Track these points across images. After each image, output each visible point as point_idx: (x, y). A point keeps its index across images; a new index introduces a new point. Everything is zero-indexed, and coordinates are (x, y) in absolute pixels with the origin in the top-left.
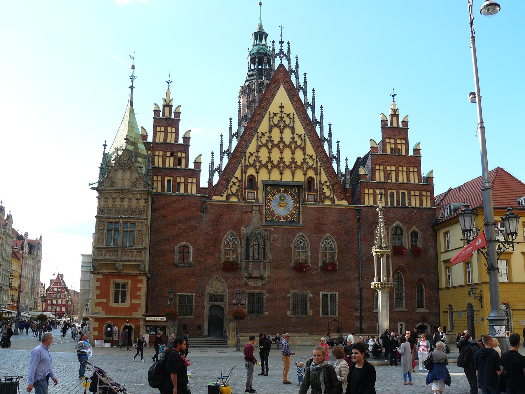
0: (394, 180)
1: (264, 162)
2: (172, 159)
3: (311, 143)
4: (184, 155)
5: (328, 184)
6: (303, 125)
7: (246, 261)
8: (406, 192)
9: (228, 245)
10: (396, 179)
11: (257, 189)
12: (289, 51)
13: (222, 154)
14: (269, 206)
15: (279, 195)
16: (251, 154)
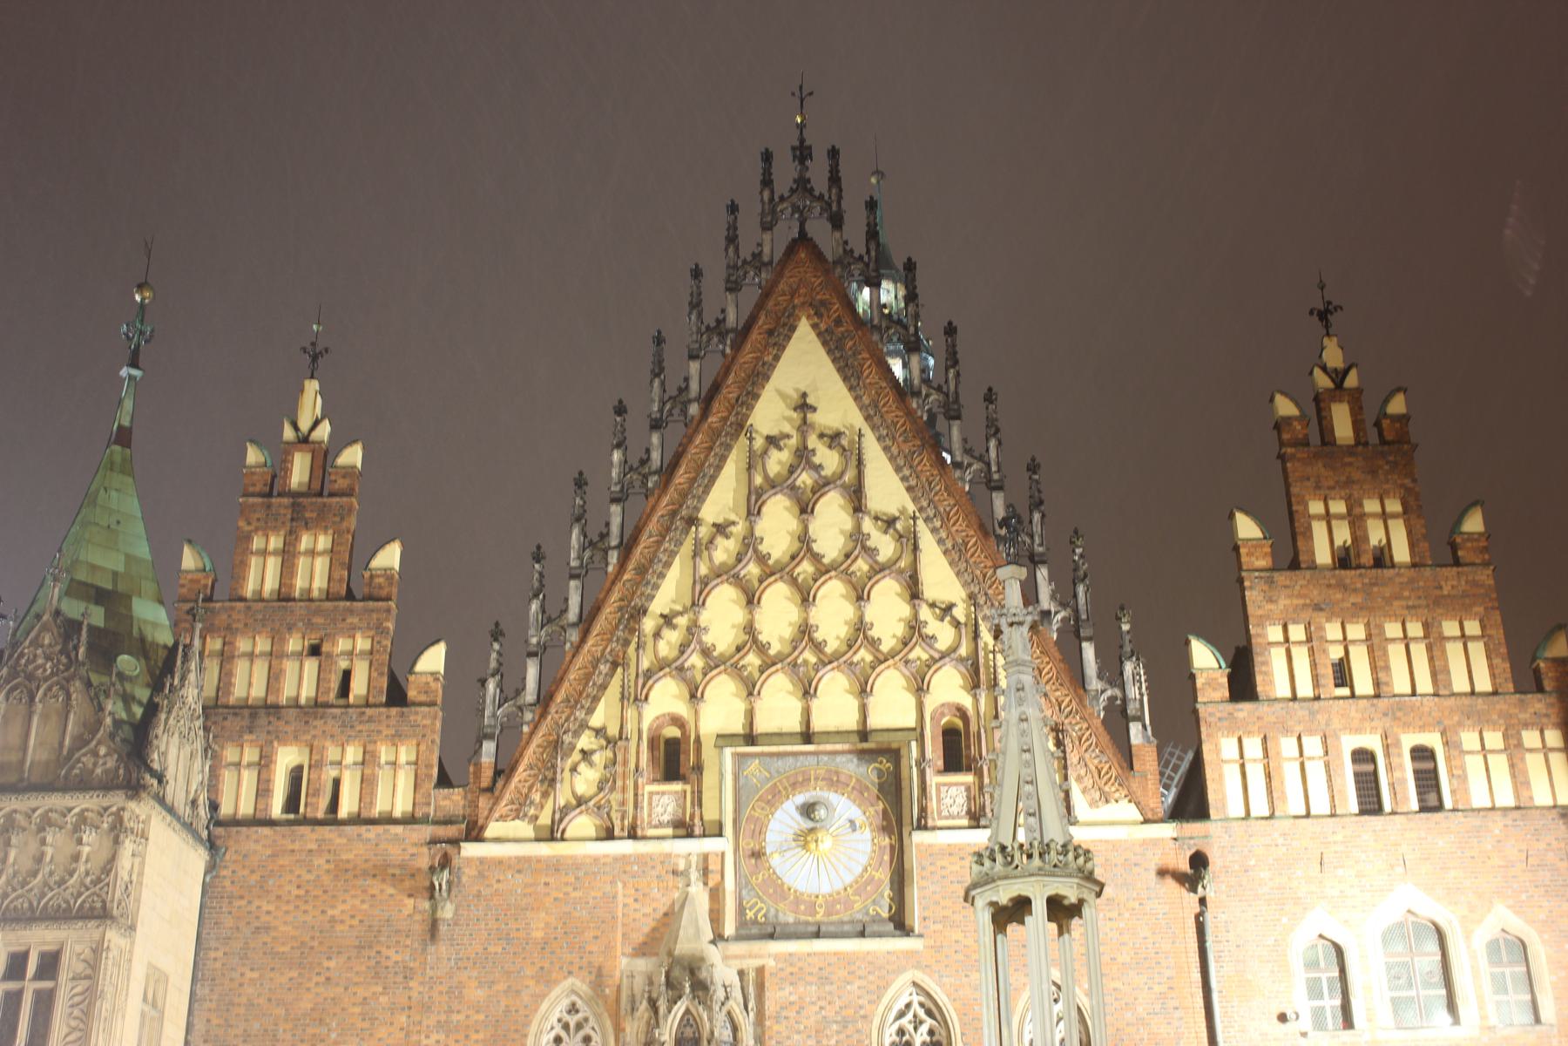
6: (903, 479)
10: (1377, 684)
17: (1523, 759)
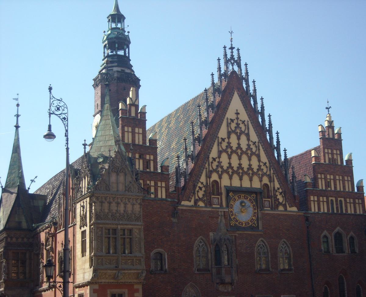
0: (333, 189)
1: (225, 168)
2: (141, 161)
3: (264, 151)
4: (152, 157)
5: (280, 191)
6: (256, 133)
7: (216, 267)
8: (343, 199)
9: (198, 250)
10: (335, 188)
11: (220, 194)
12: (239, 57)
13: (187, 157)
14: (232, 212)
15: (240, 201)
16: (214, 159)
17: (356, 205)
